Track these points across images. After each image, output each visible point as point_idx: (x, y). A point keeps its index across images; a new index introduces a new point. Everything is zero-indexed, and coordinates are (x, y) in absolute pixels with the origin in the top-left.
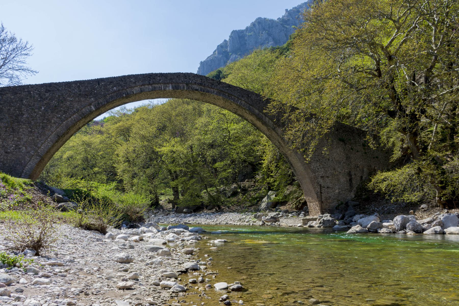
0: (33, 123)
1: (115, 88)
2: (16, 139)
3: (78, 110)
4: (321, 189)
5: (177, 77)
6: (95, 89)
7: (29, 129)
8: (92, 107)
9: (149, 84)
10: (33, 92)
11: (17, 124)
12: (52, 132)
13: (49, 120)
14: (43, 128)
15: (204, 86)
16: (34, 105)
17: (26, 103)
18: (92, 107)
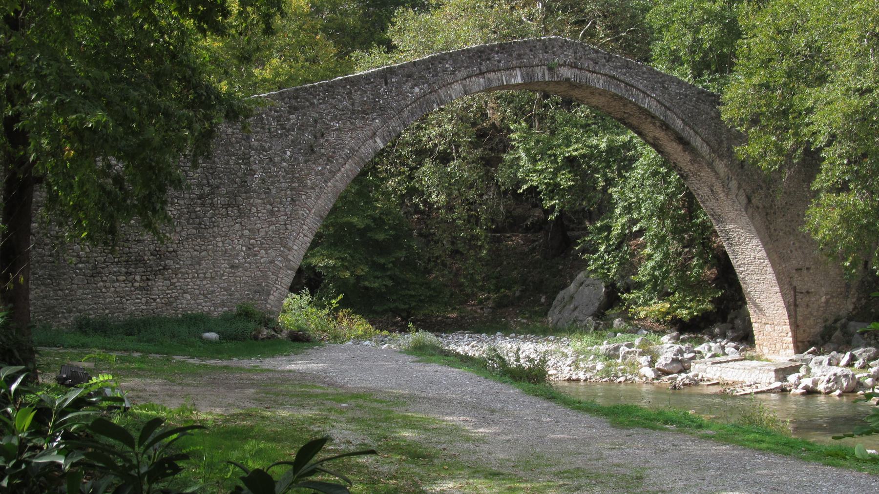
0: (274, 191)
1: (417, 90)
2: (246, 232)
3: (352, 150)
4: (795, 296)
5: (531, 51)
6: (378, 95)
7: (269, 207)
8: (378, 140)
9: (481, 73)
10: (267, 116)
11: (244, 196)
13: (301, 181)
15: (581, 69)
16: (270, 148)
17: (256, 143)
18: (378, 140)
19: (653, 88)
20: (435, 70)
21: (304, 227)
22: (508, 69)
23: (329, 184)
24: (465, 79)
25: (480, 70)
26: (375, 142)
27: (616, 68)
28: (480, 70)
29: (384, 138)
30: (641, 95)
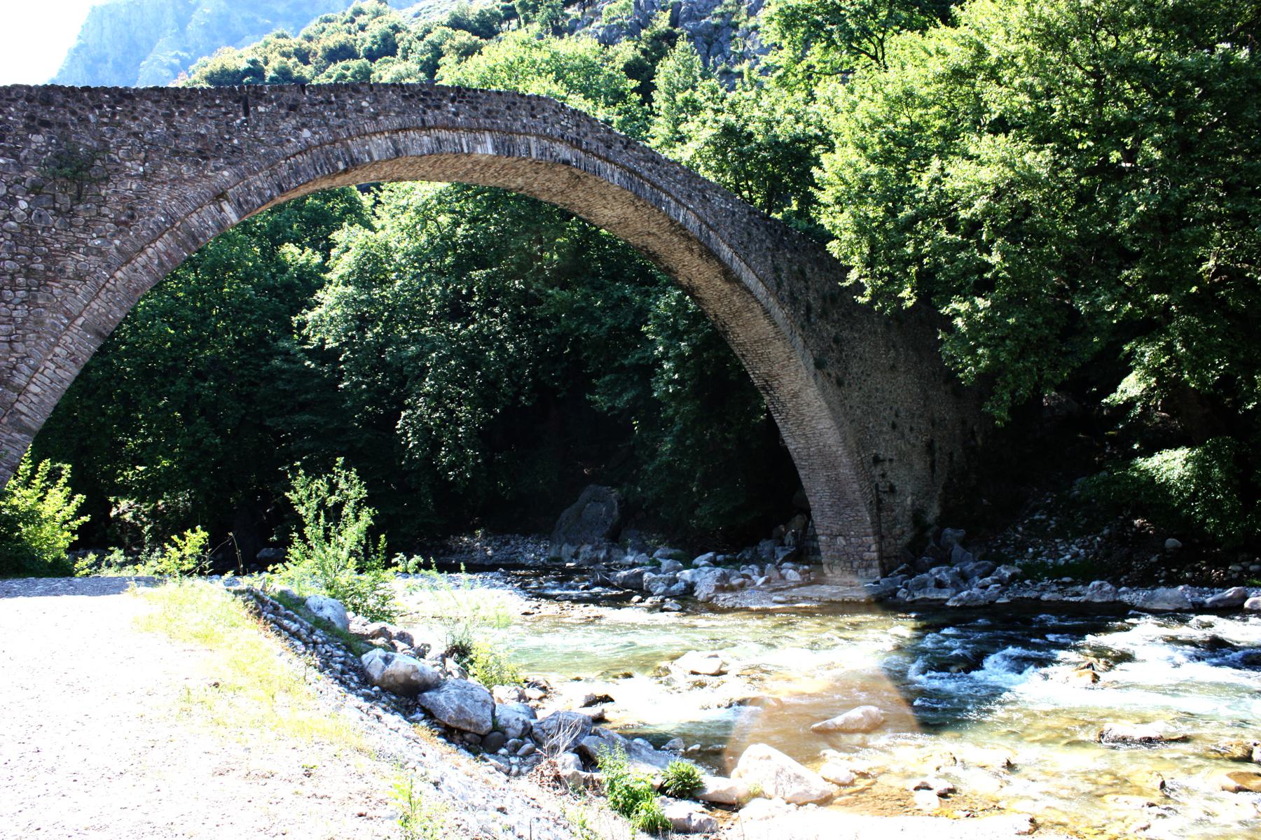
1: (306, 133)
3: (172, 218)
5: (508, 108)
9: (424, 127)
12: (72, 319)
14: (30, 301)
15: (586, 151)
18: (227, 207)
19: (689, 196)
20: (343, 107)
21: (57, 350)
22: (471, 130)
23: (119, 274)
24: (397, 131)
25: (423, 121)
26: (222, 210)
27: (637, 160)
28: (423, 121)
29: (240, 205)
30: (673, 204)
